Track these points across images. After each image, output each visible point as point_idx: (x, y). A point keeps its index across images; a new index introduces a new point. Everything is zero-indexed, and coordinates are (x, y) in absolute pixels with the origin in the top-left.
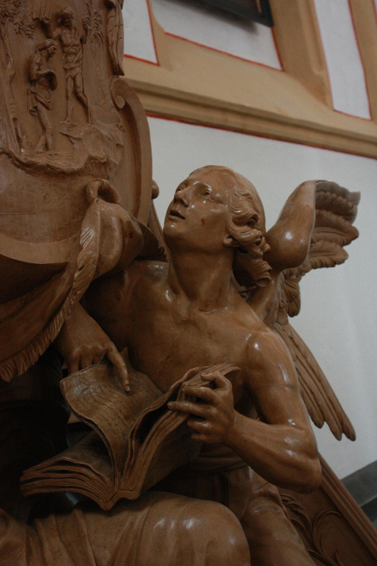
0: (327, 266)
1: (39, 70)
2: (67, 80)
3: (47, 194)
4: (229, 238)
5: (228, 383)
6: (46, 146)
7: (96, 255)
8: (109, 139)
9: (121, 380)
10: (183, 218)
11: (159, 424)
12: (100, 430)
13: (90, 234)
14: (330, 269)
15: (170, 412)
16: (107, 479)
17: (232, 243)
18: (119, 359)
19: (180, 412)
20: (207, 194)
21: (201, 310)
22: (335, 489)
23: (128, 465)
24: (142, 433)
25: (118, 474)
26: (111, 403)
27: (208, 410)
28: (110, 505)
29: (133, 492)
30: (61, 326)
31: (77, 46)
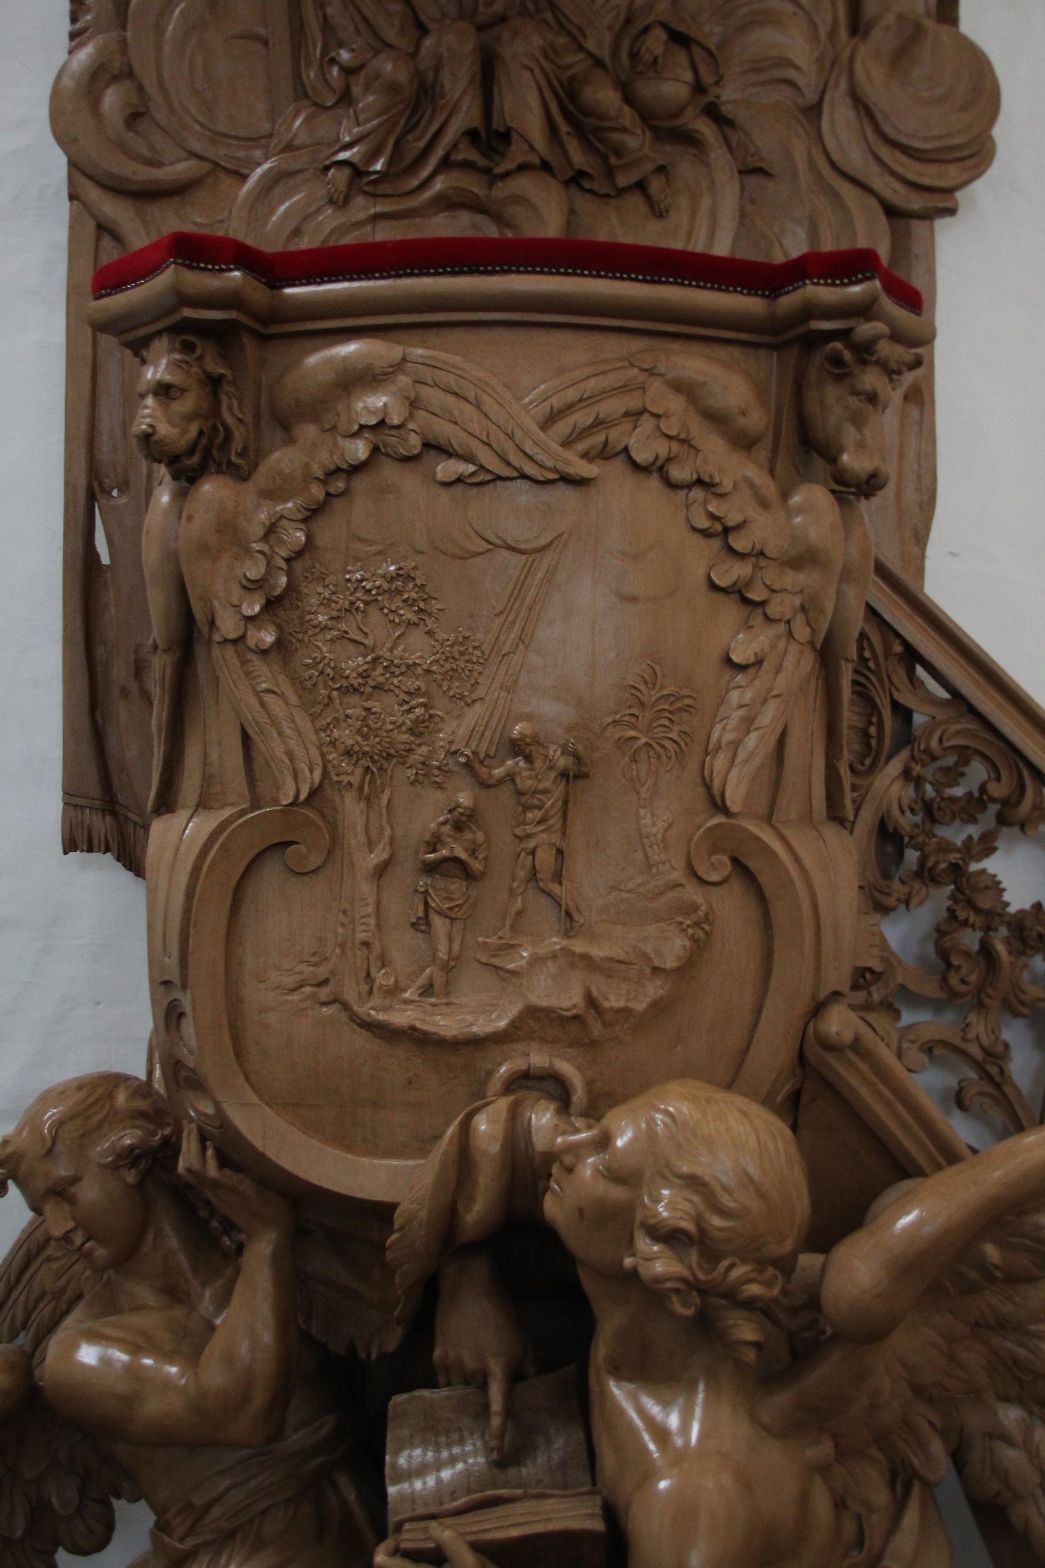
2: (518, 856)
3: (415, 1075)
6: (428, 990)
31: (545, 792)
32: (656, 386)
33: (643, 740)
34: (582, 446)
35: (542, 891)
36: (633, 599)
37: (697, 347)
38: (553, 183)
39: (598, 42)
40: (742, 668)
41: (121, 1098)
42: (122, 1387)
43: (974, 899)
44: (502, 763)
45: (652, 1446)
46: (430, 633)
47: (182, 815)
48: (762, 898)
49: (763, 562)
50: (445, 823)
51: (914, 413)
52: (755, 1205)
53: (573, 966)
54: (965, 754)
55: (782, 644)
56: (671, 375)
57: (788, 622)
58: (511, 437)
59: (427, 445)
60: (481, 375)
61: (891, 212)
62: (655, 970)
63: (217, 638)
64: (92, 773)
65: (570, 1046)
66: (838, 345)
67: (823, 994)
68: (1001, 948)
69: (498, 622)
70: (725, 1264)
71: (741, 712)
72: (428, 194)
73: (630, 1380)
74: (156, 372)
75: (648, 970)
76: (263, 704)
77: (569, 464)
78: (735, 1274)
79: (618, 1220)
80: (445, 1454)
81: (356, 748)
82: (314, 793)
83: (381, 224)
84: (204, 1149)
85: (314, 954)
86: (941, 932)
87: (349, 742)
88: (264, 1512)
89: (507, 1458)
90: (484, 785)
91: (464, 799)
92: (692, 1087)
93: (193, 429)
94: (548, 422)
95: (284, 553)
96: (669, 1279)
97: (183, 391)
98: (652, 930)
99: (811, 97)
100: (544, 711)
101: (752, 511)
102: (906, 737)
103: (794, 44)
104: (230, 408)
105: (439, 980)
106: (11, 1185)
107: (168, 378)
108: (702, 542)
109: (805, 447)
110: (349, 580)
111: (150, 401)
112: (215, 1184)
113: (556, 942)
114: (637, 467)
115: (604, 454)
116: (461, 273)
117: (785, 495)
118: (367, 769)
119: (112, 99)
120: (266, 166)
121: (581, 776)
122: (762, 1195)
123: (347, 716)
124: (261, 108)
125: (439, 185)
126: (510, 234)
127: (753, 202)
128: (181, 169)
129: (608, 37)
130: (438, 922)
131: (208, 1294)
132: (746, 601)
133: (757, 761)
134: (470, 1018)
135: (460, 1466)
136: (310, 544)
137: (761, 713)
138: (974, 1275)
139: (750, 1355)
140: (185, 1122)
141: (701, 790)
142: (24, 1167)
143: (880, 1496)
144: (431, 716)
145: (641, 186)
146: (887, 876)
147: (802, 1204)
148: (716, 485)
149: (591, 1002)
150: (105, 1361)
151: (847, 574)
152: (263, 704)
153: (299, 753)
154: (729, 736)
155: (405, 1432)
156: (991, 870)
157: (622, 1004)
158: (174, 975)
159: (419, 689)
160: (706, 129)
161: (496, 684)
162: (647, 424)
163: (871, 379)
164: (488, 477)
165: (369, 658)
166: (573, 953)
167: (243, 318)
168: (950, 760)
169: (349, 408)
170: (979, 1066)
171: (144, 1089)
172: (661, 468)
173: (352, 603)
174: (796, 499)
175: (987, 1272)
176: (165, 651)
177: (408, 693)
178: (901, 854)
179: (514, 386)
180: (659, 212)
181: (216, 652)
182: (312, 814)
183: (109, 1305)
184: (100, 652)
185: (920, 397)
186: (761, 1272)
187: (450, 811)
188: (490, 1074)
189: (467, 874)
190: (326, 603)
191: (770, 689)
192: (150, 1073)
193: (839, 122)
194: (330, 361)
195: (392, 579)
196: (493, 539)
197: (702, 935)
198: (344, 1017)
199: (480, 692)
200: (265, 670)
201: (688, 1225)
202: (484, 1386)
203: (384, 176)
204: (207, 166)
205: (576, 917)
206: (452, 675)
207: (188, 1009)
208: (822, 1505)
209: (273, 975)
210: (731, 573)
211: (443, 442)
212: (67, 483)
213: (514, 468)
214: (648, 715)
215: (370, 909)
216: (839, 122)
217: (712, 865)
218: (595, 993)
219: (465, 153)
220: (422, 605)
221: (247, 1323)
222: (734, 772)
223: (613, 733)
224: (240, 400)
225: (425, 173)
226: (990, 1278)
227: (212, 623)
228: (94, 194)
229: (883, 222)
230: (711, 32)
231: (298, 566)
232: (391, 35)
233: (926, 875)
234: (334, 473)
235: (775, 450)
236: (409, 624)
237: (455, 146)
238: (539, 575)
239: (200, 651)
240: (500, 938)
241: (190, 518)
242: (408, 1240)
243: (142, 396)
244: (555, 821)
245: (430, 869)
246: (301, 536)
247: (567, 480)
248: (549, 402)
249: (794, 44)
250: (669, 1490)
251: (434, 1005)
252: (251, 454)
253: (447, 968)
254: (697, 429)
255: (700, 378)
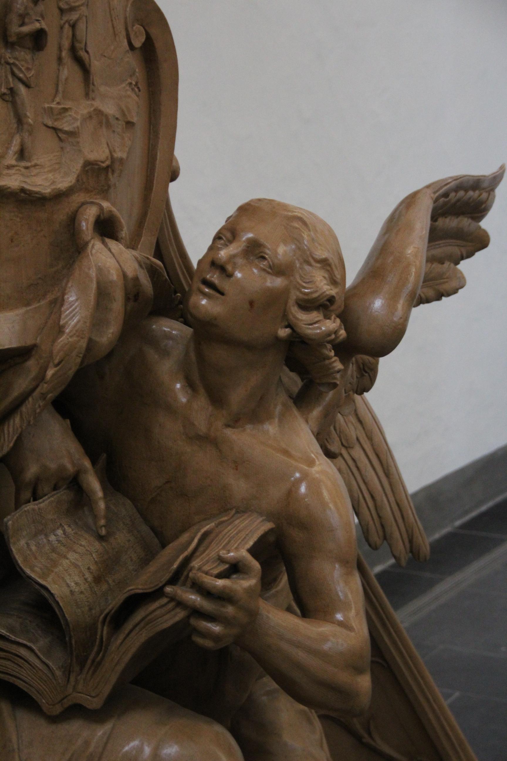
0: (428, 301)
1: (23, 24)
2: (62, 28)
3: (16, 233)
4: (286, 327)
5: (256, 565)
6: (22, 154)
7: (83, 344)
8: (117, 119)
9: (95, 517)
10: (222, 294)
11: (147, 612)
12: (57, 603)
13: (76, 309)
14: (435, 304)
15: (164, 600)
16: (58, 673)
17: (290, 336)
18: (94, 484)
19: (180, 604)
20: (264, 258)
21: (228, 426)
22: (384, 625)
23: (93, 661)
24: (120, 616)
25: (77, 668)
26: (76, 556)
27: (224, 610)
28: (57, 710)
29: (95, 700)
30: (15, 438)
240: (58, 103)
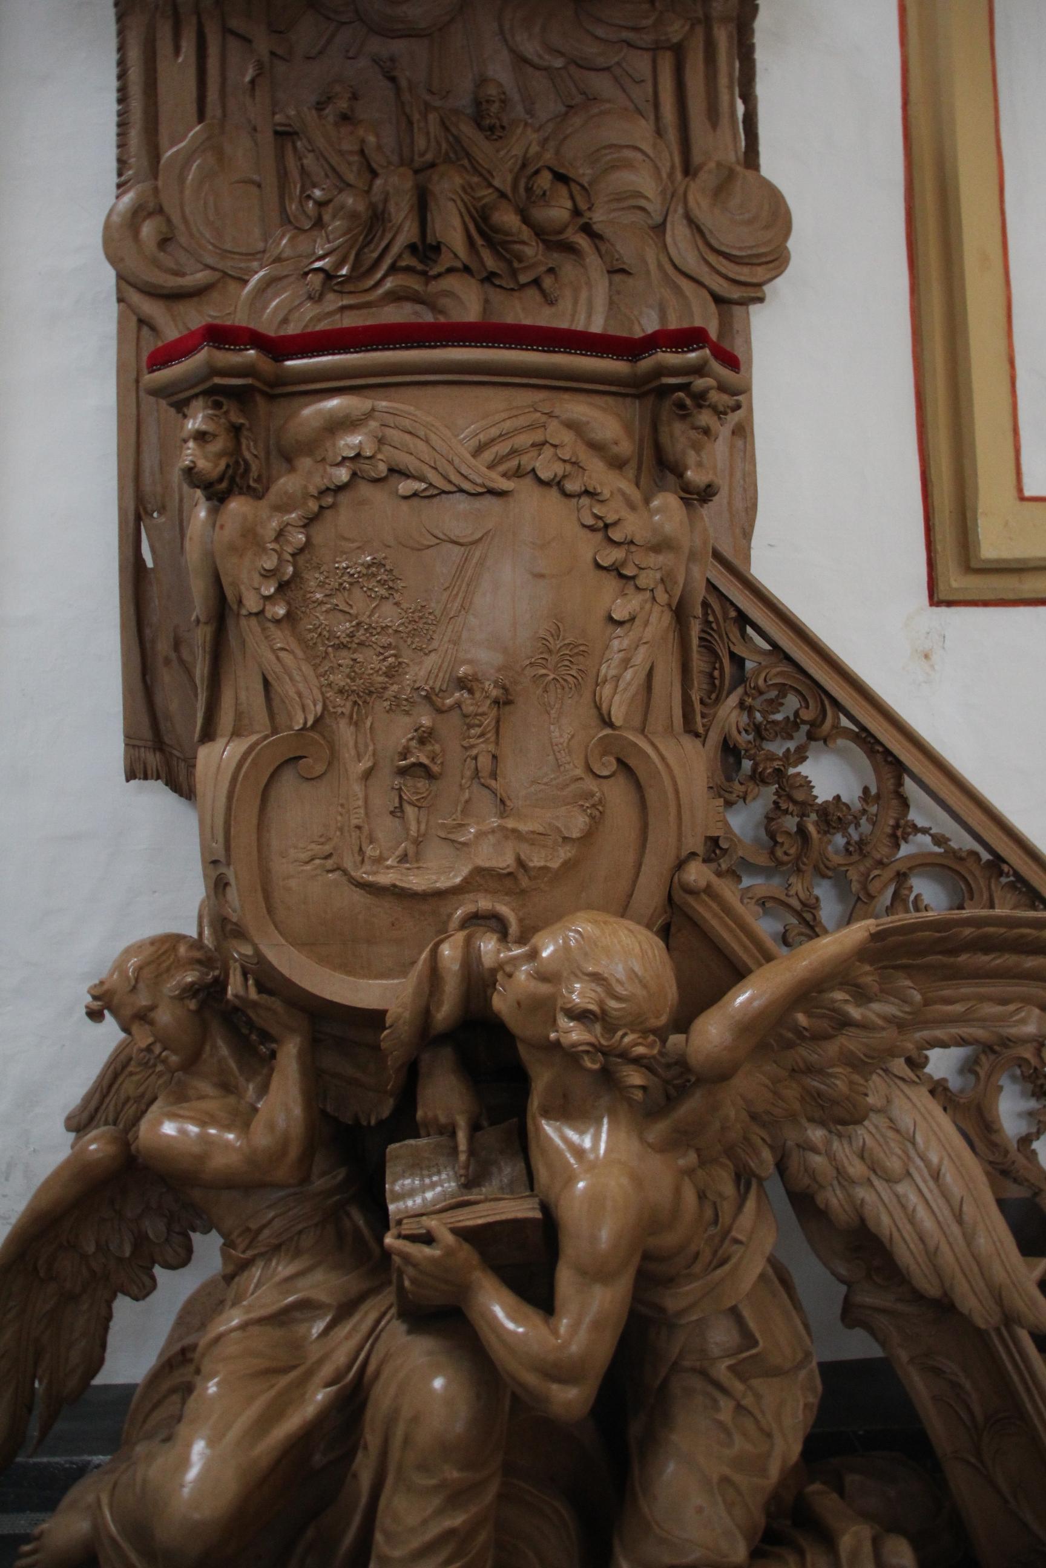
6: (404, 858)
31: (483, 714)
32: (553, 425)
33: (552, 676)
34: (502, 468)
35: (483, 785)
36: (542, 576)
37: (582, 397)
38: (473, 281)
39: (502, 180)
40: (620, 623)
41: (182, 950)
42: (196, 1149)
43: (792, 794)
44: (452, 695)
45: (572, 1161)
46: (397, 604)
47: (220, 742)
48: (639, 787)
49: (633, 548)
50: (412, 739)
51: (740, 443)
52: (640, 992)
53: (506, 838)
54: (783, 690)
55: (648, 606)
56: (564, 416)
57: (652, 590)
58: (451, 462)
59: (392, 470)
60: (429, 419)
61: (718, 300)
62: (565, 838)
63: (244, 612)
64: (145, 720)
65: (507, 894)
66: (681, 394)
67: (684, 854)
68: (812, 828)
69: (446, 594)
70: (620, 1033)
71: (621, 655)
72: (381, 291)
73: (556, 1120)
74: (195, 423)
75: (560, 840)
76: (278, 658)
77: (493, 481)
78: (626, 1040)
79: (544, 1008)
80: (427, 1181)
81: (347, 688)
82: (318, 721)
83: (347, 313)
84: (246, 980)
85: (321, 836)
86: (769, 819)
87: (342, 684)
88: (300, 1232)
89: (470, 1183)
90: (440, 711)
91: (426, 721)
92: (594, 914)
93: (223, 463)
94: (478, 452)
95: (290, 550)
96: (581, 1045)
97: (215, 436)
98: (563, 810)
99: (659, 219)
100: (482, 657)
101: (625, 513)
102: (740, 678)
103: (644, 181)
104: (249, 449)
105: (411, 852)
106: (106, 1012)
107: (204, 427)
108: (590, 535)
109: (661, 467)
110: (337, 568)
111: (191, 444)
112: (255, 1005)
113: (494, 822)
114: (541, 482)
115: (518, 473)
116: (412, 347)
117: (647, 501)
118: (355, 703)
119: (148, 230)
120: (261, 273)
121: (509, 703)
122: (645, 986)
123: (340, 665)
124: (257, 232)
125: (388, 284)
126: (442, 319)
127: (618, 293)
128: (201, 277)
129: (509, 178)
130: (410, 810)
131: (251, 1087)
132: (622, 576)
133: (633, 689)
134: (434, 877)
135: (439, 1189)
136: (308, 546)
137: (635, 655)
138: (790, 1035)
139: (639, 1095)
140: (231, 962)
141: (594, 711)
142: (116, 1001)
143: (728, 1189)
144: (400, 663)
145: (536, 282)
146: (729, 779)
147: (672, 992)
148: (598, 494)
149: (521, 863)
150: (182, 1132)
151: (692, 556)
152: (278, 658)
153: (305, 692)
154: (612, 672)
155: (399, 1169)
156: (804, 774)
157: (542, 864)
158: (220, 855)
159: (390, 644)
160: (583, 242)
161: (446, 639)
162: (548, 452)
163: (705, 418)
164: (436, 492)
165: (354, 623)
166: (507, 829)
167: (258, 384)
168: (773, 694)
169: (334, 445)
170: (798, 914)
171: (197, 944)
172: (559, 483)
173: (341, 584)
174: (655, 503)
175: (798, 1032)
176: (206, 623)
177: (383, 647)
178: (740, 763)
179: (452, 427)
180: (550, 300)
181: (243, 622)
182: (316, 736)
183: (181, 1096)
184: (148, 631)
185: (743, 432)
186: (645, 1038)
187: (416, 730)
188: (450, 916)
189: (430, 775)
190: (322, 585)
191: (641, 638)
192: (201, 934)
193: (678, 235)
194: (320, 411)
195: (369, 566)
196: (441, 536)
197: (597, 813)
198: (344, 879)
199: (435, 644)
200: (279, 633)
201: (593, 1007)
202: (453, 1135)
203: (348, 278)
204: (218, 275)
205: (508, 803)
206: (413, 634)
207: (233, 881)
208: (690, 1196)
209: (292, 851)
210: (613, 555)
211: (402, 467)
212: (120, 508)
213: (455, 485)
214: (553, 659)
215: (360, 803)
216: (678, 235)
217: (603, 764)
218: (523, 857)
219: (408, 261)
220: (391, 584)
221: (282, 1104)
222: (617, 698)
223: (530, 672)
224: (255, 442)
225: (379, 275)
226: (803, 1038)
227: (240, 602)
228: (135, 298)
229: (712, 307)
230: (584, 173)
231: (301, 560)
232: (351, 178)
233: (758, 778)
234: (324, 492)
235: (639, 468)
236: (383, 598)
237: (400, 256)
238: (474, 561)
239: (230, 623)
241: (222, 527)
242: (395, 1040)
243: (185, 441)
244: (491, 735)
245: (402, 772)
246: (302, 538)
247: (491, 492)
248: (477, 438)
249: (644, 181)
250: (585, 1188)
251: (408, 869)
252: (264, 481)
253: (417, 843)
254: (584, 455)
255: (584, 419)
